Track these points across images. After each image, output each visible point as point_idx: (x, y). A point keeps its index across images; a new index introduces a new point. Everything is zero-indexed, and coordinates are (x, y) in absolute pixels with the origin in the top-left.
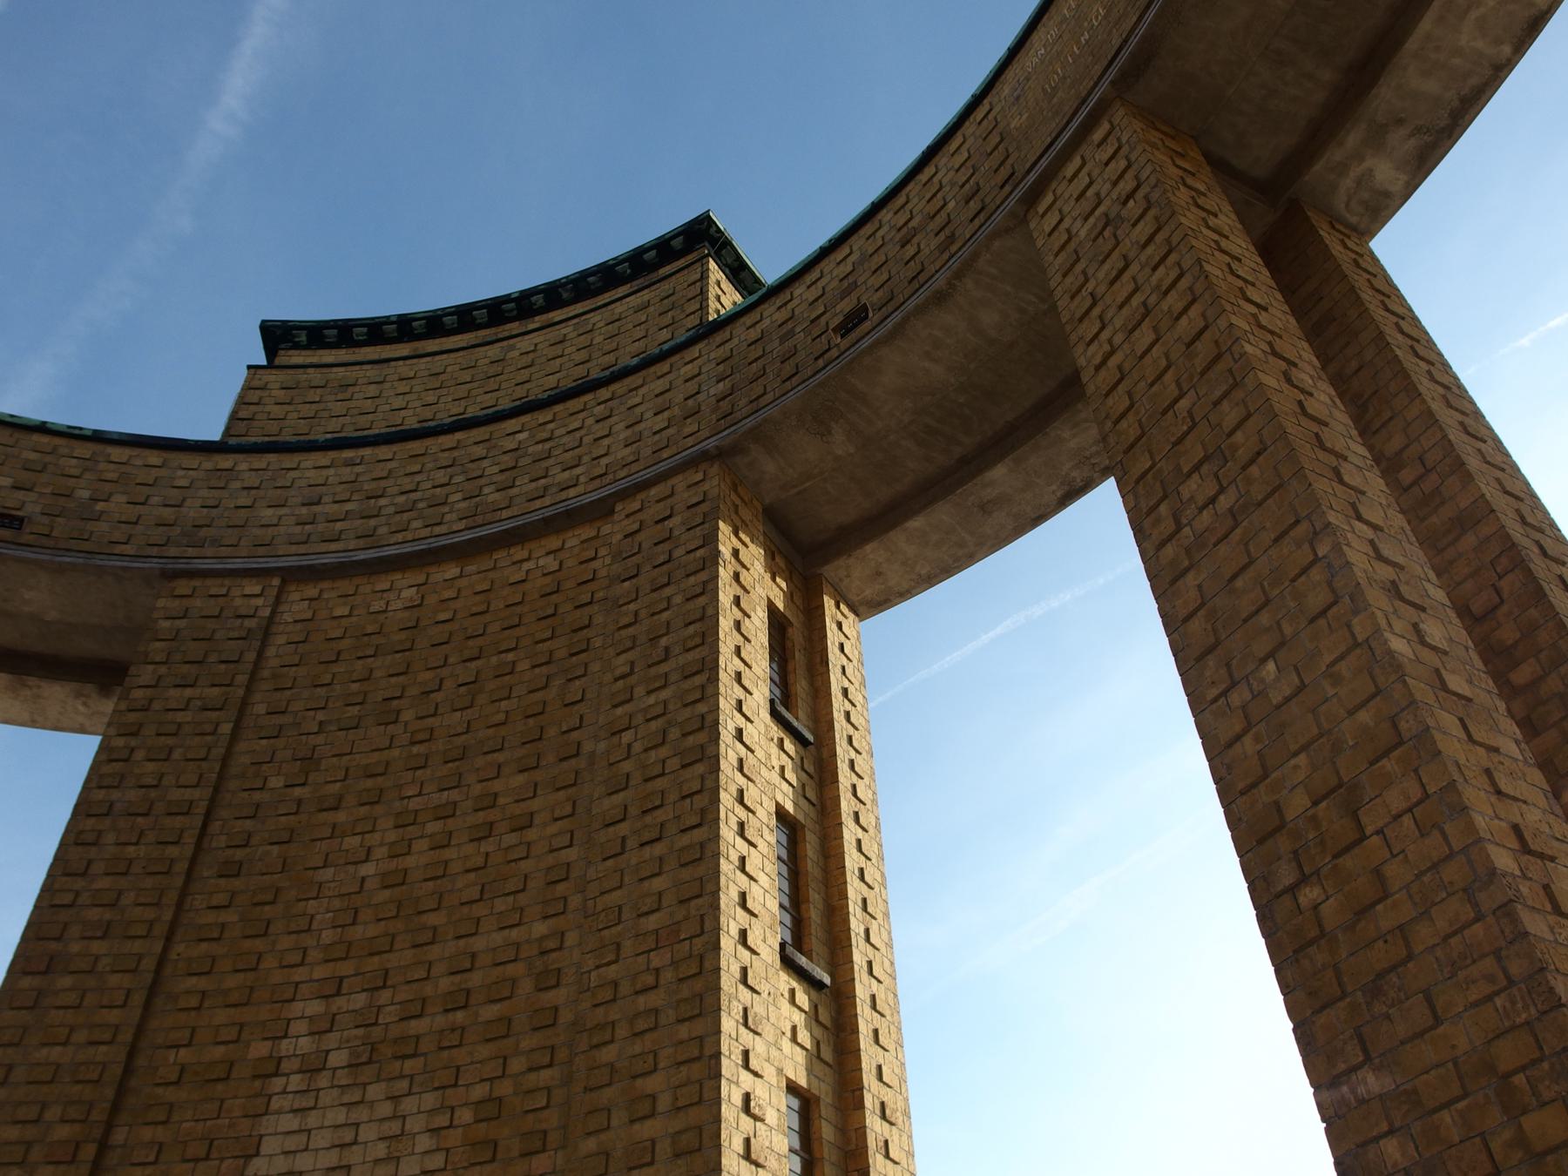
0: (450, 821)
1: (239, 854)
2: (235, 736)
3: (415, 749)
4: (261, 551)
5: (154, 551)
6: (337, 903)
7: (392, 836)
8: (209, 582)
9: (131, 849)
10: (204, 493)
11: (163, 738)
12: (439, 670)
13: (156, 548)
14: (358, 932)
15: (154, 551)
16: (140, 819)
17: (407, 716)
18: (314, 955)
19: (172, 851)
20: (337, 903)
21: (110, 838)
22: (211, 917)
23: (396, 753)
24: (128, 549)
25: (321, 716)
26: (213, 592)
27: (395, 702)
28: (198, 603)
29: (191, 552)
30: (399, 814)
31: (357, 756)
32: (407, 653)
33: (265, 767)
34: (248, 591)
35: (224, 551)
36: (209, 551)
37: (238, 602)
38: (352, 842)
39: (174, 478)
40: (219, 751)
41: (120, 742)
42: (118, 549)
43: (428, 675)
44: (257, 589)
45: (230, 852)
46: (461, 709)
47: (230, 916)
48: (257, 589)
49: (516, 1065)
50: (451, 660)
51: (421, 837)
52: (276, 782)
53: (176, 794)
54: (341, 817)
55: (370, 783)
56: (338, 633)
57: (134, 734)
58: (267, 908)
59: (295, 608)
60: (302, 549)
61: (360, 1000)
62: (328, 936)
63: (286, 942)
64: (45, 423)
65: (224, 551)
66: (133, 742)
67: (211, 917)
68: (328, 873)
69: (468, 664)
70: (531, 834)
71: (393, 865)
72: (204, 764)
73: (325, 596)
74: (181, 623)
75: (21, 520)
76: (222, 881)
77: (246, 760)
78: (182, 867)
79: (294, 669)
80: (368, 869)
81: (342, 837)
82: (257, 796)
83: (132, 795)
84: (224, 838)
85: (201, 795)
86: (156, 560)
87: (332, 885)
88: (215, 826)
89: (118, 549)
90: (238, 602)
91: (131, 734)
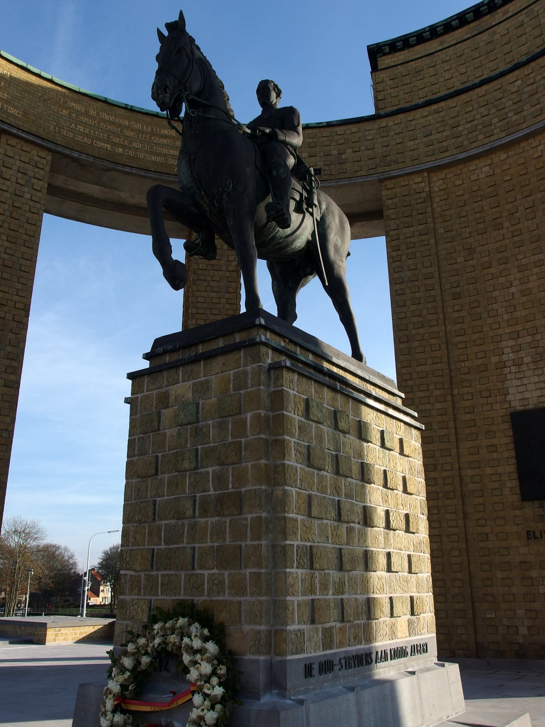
0: (542, 267)
1: (457, 290)
3: (516, 239)
4: (416, 162)
5: (373, 171)
6: (505, 304)
7: (518, 276)
8: (399, 180)
9: (417, 294)
10: (380, 140)
11: (410, 249)
12: (514, 203)
13: (373, 170)
15: (373, 171)
16: (415, 282)
17: (506, 225)
18: (503, 324)
19: (433, 293)
20: (505, 304)
21: (408, 291)
22: (456, 315)
23: (507, 241)
24: (363, 173)
25: (468, 230)
26: (402, 184)
27: (499, 220)
28: (398, 190)
29: (387, 169)
30: (518, 267)
31: (491, 245)
32: (496, 197)
33: (453, 254)
34: (416, 181)
35: (401, 165)
36: (395, 167)
37: (414, 186)
38: (502, 280)
39: (366, 136)
41: (394, 254)
42: (359, 174)
43: (509, 206)
44: (420, 179)
45: (453, 289)
46: (531, 219)
47: (464, 314)
48: (420, 179)
50: (518, 198)
51: (532, 275)
52: (461, 260)
53: (424, 271)
54: (493, 270)
55: (500, 255)
56: (461, 193)
57: (398, 250)
58: (477, 309)
59: (437, 184)
60: (433, 158)
62: (506, 317)
63: (490, 321)
64: (307, 124)
65: (401, 165)
66: (400, 253)
67: (456, 315)
68: (497, 293)
69: (527, 199)
71: (523, 287)
72: (430, 257)
73: (448, 177)
74: (396, 200)
76: (455, 301)
78: (439, 298)
79: (448, 211)
80: (513, 290)
81: (498, 278)
82: (455, 266)
83: (409, 273)
84: (449, 284)
86: (375, 175)
87: (500, 297)
88: (444, 280)
89: (359, 174)
90: (414, 186)
91: (398, 250)
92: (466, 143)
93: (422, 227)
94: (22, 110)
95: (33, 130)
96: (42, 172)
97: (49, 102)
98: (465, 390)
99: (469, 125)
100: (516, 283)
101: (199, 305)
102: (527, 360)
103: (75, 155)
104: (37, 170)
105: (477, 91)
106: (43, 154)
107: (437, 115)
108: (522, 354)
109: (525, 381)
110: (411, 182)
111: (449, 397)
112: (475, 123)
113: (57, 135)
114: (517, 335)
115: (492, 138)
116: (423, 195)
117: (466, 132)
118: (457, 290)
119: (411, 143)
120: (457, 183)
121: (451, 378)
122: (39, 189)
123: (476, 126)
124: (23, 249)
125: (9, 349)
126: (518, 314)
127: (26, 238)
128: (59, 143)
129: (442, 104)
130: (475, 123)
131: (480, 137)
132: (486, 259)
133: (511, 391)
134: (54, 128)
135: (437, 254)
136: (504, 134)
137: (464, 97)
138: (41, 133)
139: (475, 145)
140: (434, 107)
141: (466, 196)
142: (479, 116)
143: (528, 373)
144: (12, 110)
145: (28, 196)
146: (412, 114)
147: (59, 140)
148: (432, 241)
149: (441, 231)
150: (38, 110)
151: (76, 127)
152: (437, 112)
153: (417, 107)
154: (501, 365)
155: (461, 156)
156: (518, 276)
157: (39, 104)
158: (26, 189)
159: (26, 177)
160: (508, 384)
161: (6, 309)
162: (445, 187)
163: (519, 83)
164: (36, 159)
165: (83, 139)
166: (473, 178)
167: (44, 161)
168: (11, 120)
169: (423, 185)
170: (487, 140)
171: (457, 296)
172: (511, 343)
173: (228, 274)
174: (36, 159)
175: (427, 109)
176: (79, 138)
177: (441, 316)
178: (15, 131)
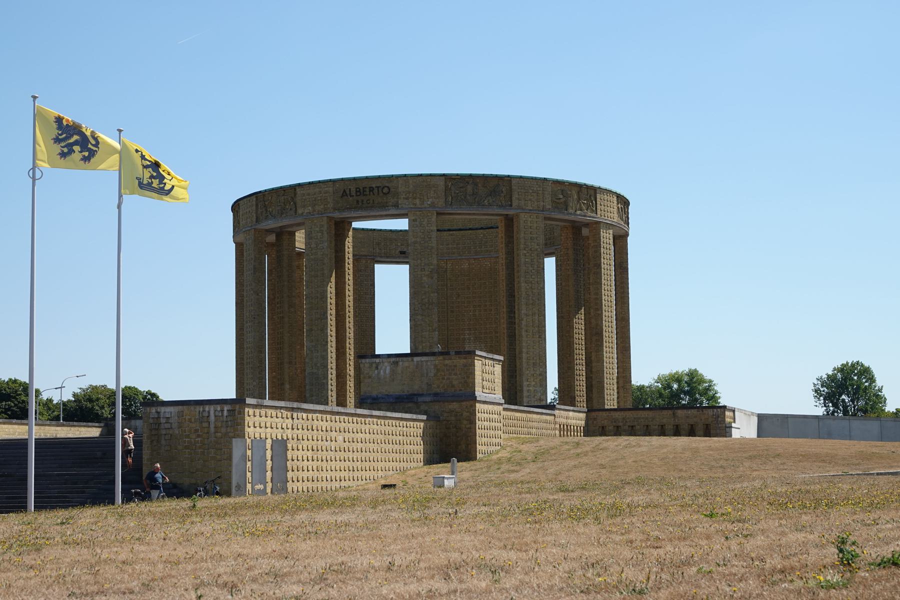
2: (447, 290)
7: (473, 309)
14: (471, 322)
17: (471, 289)
20: (467, 318)
23: (471, 295)
40: (445, 294)
49: (494, 342)
52: (455, 298)
61: (473, 332)
62: (467, 323)
63: (462, 323)
70: (492, 312)
75: (405, 252)
77: (449, 294)
85: (446, 301)
92: (461, 253)
93: (442, 283)
98: (452, 346)
99: (463, 246)
100: (472, 311)
101: (361, 309)
102: (472, 339)
105: (468, 231)
107: (452, 237)
108: (471, 336)
109: (470, 346)
110: (440, 263)
111: (447, 348)
112: (465, 245)
114: (469, 330)
115: (471, 254)
116: (444, 269)
117: (461, 248)
118: (452, 309)
119: (442, 246)
120: (457, 267)
121: (448, 341)
123: (465, 247)
126: (471, 322)
129: (454, 232)
130: (465, 245)
131: (467, 252)
132: (463, 300)
133: (466, 348)
135: (447, 295)
136: (474, 254)
137: (462, 232)
139: (464, 255)
140: (451, 232)
141: (459, 274)
142: (467, 243)
143: (472, 343)
146: (443, 232)
148: (446, 289)
149: (449, 285)
152: (451, 235)
153: (445, 231)
154: (464, 339)
155: (459, 258)
156: (473, 309)
160: (465, 346)
162: (452, 267)
163: (482, 235)
166: (462, 267)
169: (444, 265)
170: (468, 255)
171: (452, 312)
172: (468, 332)
173: (371, 296)
175: (448, 232)
177: (446, 319)
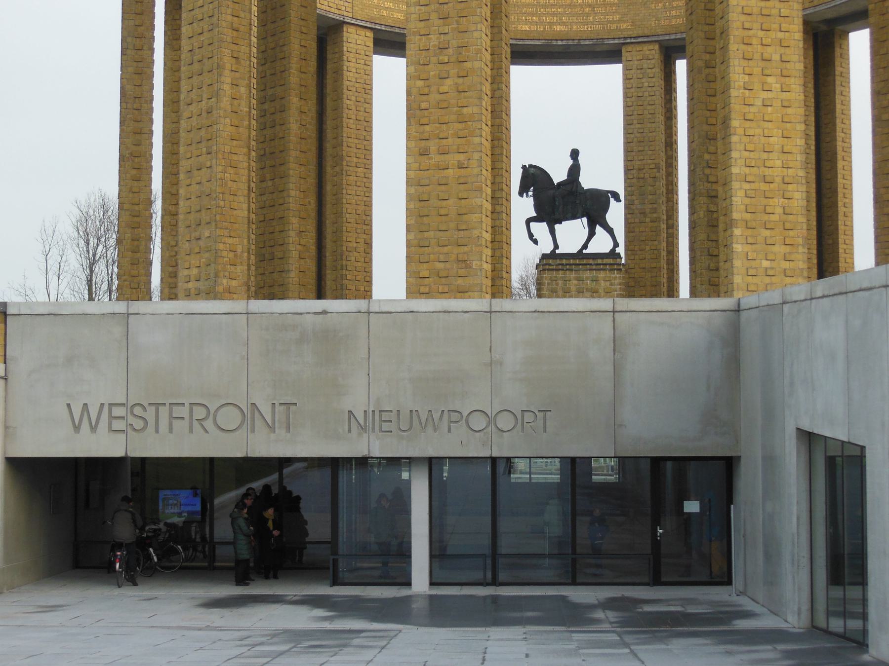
94: (630, 21)
95: (640, 33)
96: (653, 62)
97: (648, 3)
103: (673, 37)
104: (649, 61)
106: (651, 47)
113: (657, 27)
122: (652, 76)
124: (649, 125)
125: (650, 197)
127: (650, 116)
128: (660, 33)
134: (655, 23)
138: (647, 32)
144: (624, 26)
145: (646, 85)
147: (659, 31)
150: (642, 15)
151: (670, 14)
157: (641, 9)
158: (643, 80)
159: (643, 71)
161: (644, 171)
164: (648, 52)
165: (676, 22)
167: (653, 52)
168: (625, 34)
174: (648, 52)
176: (674, 22)
178: (628, 41)
